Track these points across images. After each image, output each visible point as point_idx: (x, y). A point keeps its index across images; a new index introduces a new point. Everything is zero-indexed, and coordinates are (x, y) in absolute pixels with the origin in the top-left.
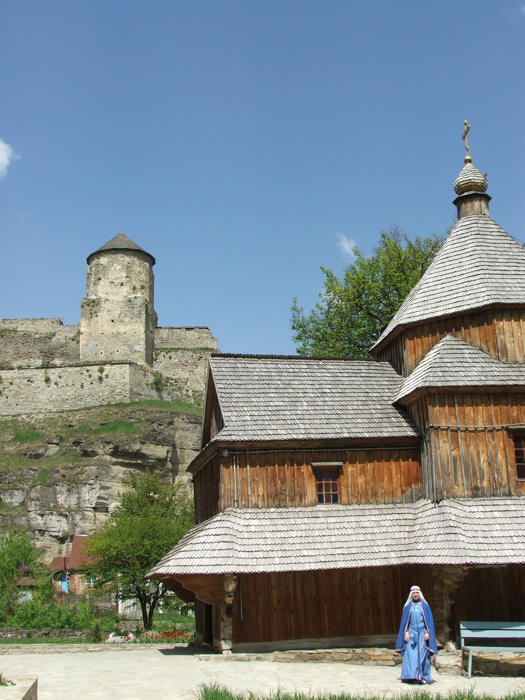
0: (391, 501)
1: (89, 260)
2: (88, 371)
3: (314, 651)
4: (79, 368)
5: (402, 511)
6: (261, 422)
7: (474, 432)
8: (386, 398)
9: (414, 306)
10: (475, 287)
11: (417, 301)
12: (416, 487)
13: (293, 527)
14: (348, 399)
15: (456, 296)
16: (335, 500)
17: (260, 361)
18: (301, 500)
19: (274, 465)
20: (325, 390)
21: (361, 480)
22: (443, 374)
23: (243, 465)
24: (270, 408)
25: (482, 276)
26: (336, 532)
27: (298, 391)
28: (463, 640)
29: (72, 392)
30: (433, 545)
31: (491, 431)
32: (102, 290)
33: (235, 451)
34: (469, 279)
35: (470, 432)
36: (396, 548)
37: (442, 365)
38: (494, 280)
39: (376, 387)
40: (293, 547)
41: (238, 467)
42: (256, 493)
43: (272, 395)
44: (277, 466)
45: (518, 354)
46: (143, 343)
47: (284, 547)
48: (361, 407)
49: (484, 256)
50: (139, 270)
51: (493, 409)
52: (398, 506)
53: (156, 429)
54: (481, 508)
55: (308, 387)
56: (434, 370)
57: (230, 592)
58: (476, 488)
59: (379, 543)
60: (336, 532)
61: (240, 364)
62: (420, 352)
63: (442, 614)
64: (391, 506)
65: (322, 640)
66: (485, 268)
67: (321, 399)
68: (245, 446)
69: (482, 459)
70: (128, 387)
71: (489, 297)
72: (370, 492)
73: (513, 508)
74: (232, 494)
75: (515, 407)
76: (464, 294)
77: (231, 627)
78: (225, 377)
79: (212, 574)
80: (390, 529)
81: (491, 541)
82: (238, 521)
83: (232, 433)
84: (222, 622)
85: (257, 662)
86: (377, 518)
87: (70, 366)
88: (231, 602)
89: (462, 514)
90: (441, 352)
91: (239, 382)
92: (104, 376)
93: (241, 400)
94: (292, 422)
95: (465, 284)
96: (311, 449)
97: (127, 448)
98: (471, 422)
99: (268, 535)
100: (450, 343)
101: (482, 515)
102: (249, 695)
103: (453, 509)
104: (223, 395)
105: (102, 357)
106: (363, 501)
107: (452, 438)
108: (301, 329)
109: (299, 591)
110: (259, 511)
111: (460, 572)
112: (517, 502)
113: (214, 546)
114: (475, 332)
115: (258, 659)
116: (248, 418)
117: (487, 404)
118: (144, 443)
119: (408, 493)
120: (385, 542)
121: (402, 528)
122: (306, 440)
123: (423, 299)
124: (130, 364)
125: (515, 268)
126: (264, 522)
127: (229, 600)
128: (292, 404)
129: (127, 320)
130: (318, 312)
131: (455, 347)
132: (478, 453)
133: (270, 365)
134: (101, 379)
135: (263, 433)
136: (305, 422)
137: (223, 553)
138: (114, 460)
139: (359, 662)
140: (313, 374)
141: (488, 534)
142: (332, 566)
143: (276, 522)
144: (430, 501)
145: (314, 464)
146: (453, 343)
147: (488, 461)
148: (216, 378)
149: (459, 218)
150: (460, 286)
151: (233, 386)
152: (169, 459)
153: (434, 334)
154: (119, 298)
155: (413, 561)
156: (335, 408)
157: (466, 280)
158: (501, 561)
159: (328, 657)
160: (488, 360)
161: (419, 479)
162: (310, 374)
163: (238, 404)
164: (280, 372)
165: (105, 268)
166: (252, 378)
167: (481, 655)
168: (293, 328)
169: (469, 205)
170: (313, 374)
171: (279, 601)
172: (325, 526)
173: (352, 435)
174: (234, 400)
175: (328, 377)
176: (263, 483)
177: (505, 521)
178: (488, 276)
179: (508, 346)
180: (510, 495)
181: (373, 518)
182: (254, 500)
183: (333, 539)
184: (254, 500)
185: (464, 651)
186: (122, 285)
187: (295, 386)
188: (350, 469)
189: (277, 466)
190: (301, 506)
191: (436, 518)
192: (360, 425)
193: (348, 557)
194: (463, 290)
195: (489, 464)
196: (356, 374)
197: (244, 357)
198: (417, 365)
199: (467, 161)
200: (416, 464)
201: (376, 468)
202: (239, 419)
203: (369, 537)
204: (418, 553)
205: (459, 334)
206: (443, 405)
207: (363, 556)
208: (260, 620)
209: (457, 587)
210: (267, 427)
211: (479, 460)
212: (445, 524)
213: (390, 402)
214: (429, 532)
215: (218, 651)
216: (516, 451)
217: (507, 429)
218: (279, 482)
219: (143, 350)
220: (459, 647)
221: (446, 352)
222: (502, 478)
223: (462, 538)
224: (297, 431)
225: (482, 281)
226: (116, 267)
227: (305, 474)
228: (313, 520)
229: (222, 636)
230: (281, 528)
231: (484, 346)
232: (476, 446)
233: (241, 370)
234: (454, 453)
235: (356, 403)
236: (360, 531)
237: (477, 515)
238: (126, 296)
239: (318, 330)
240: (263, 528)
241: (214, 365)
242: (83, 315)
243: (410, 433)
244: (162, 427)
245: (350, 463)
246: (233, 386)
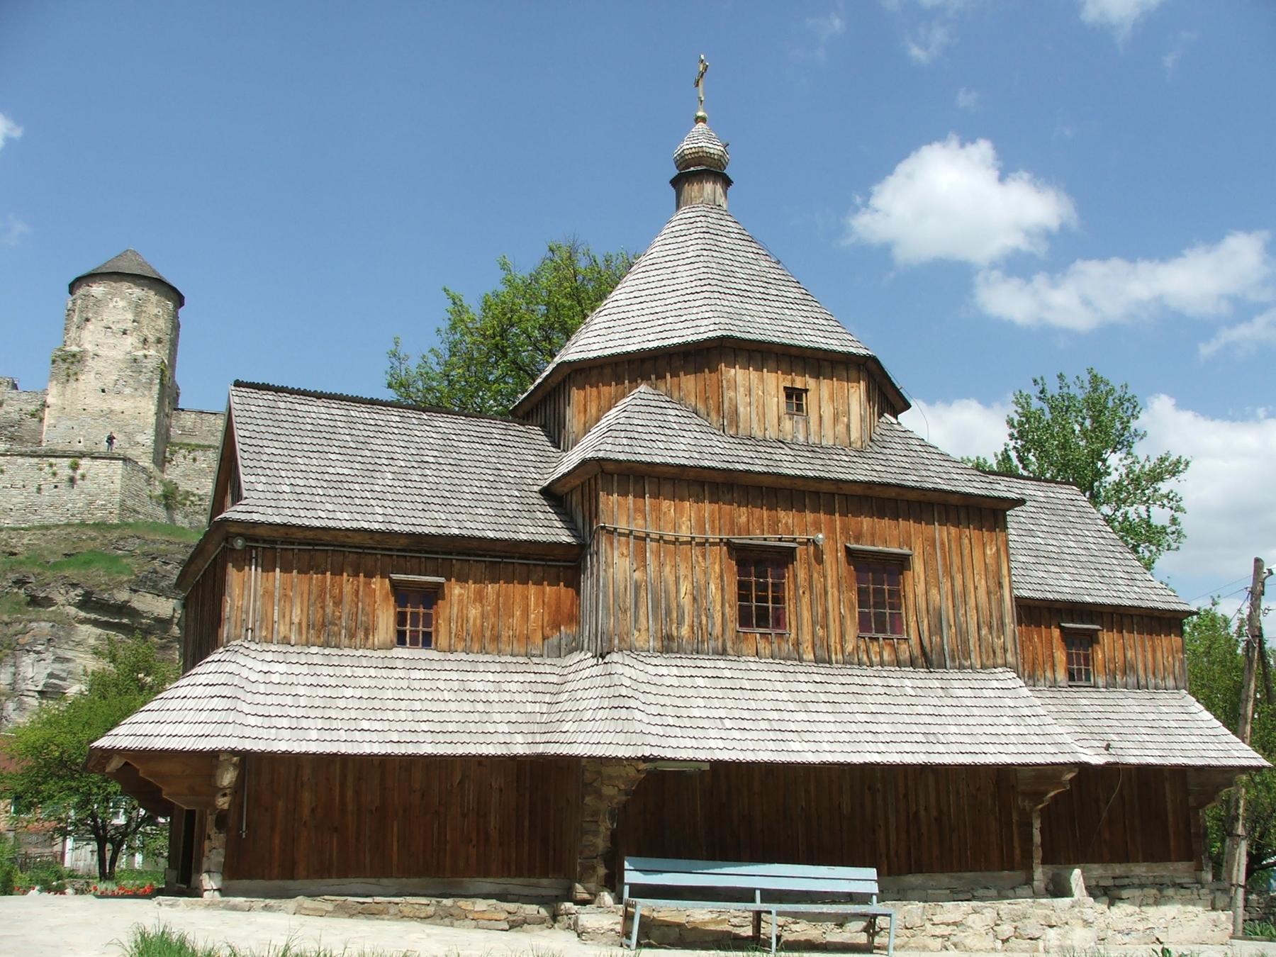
0: (523, 651)
1: (73, 287)
2: (51, 465)
3: (369, 900)
4: (36, 460)
5: (541, 669)
6: (308, 498)
7: (674, 543)
8: (530, 482)
9: (590, 334)
10: (695, 310)
11: (597, 327)
12: (569, 631)
13: (347, 682)
14: (465, 476)
15: (661, 322)
16: (427, 641)
17: (319, 402)
18: (367, 637)
19: (324, 573)
20: (426, 459)
21: (474, 612)
22: (630, 442)
23: (268, 568)
24: (327, 477)
25: (707, 295)
26: (423, 695)
27: (379, 454)
28: (627, 889)
29: (21, 499)
30: (589, 726)
31: (702, 544)
32: (89, 338)
33: (257, 541)
34: (686, 298)
35: (666, 542)
36: (525, 728)
37: (629, 428)
38: (726, 303)
39: (514, 462)
40: (345, 714)
41: (259, 570)
42: (287, 619)
43: (333, 457)
44: (328, 574)
45: (755, 425)
46: (151, 432)
47: (328, 713)
48: (485, 491)
49: (714, 265)
50: (156, 311)
51: (707, 508)
52: (535, 660)
53: (158, 569)
54: (675, 671)
55: (398, 450)
56: (615, 434)
57: (225, 788)
58: (670, 637)
59: (497, 717)
60: (423, 695)
61: (284, 403)
62: (593, 410)
63: (595, 846)
64: (522, 660)
65: (385, 881)
66: (713, 282)
67: (419, 472)
68: (275, 534)
69: (683, 590)
70: (117, 498)
71: (716, 327)
72: (488, 634)
73: (728, 673)
74: (244, 616)
75: (743, 509)
76: (676, 319)
77: (222, 851)
78: (254, 421)
79: (194, 751)
80: (517, 697)
81: (687, 722)
82: (250, 663)
83: (255, 509)
84: (207, 842)
85: (264, 913)
86: (497, 677)
87: (22, 455)
88: (226, 806)
89: (642, 677)
90: (629, 408)
91: (278, 431)
92: (78, 477)
93: (278, 458)
94: (363, 502)
95: (679, 305)
96: (391, 550)
97: (106, 596)
98: (670, 526)
99: (301, 690)
100: (645, 396)
101: (675, 682)
102: (228, 951)
103: (624, 668)
104: (245, 448)
105: (80, 447)
106: (476, 647)
107: (635, 550)
108: (399, 384)
109: (350, 793)
110: (291, 649)
111: (632, 773)
112: (735, 665)
113: (203, 704)
114: (689, 382)
115: (267, 908)
116: (287, 489)
117: (699, 499)
118: (135, 591)
119: (554, 640)
120: (507, 718)
121: (539, 697)
122: (383, 532)
123: (606, 325)
124: (125, 460)
125: (762, 290)
126: (297, 669)
127: (223, 802)
128: (367, 473)
129: (127, 391)
130: (432, 360)
131: (653, 403)
132: (677, 579)
133: (336, 410)
134: (72, 480)
135: (309, 514)
136: (385, 503)
137: (216, 716)
138: (82, 614)
139: (447, 921)
140: (408, 432)
141: (684, 712)
142: (410, 750)
143: (319, 670)
144: (589, 654)
145: (395, 576)
146: (651, 397)
147: (692, 594)
148: (238, 420)
149: (678, 207)
150: (670, 307)
151: (266, 435)
152: (176, 620)
153: (619, 381)
154: (119, 354)
155: (552, 750)
156: (440, 487)
157: (681, 299)
158: (702, 755)
159: (392, 911)
160: (705, 429)
161: (574, 618)
162: (403, 431)
163: (271, 465)
164: (352, 422)
165: (98, 303)
166: (302, 426)
167: (655, 914)
168: (390, 386)
169: (696, 187)
170: (408, 432)
171: (313, 811)
172: (404, 684)
173: (464, 532)
174: (265, 457)
175: (434, 438)
176: (302, 603)
177: (713, 693)
178: (716, 295)
179: (741, 409)
180: (724, 652)
181: (490, 677)
182: (282, 629)
183: (418, 705)
184: (282, 629)
185: (627, 905)
186: (125, 333)
187: (375, 447)
188: (456, 590)
189: (328, 574)
190: (365, 647)
191: (598, 682)
192: (481, 518)
193: (441, 738)
194: (674, 313)
195: (694, 599)
196: (482, 439)
197: (292, 392)
198: (586, 431)
199: (698, 120)
200: (571, 591)
201: (503, 592)
202: (270, 488)
203: (480, 707)
204: (562, 738)
205: (661, 384)
206: (624, 494)
207: (466, 738)
208: (277, 841)
209: (624, 798)
210: (319, 506)
211: (678, 591)
212: (612, 691)
213: (536, 488)
214: (583, 705)
215: (196, 892)
216: (739, 582)
217: (728, 543)
218: (330, 603)
219: (149, 443)
220: (619, 899)
221: (637, 409)
222: (713, 624)
223: (638, 715)
224: (370, 517)
225: (706, 301)
226: (118, 304)
227: (378, 592)
228: (385, 673)
229: (205, 867)
230: (327, 681)
231: (701, 407)
232: (675, 566)
233: (284, 412)
234: (637, 575)
235: (477, 483)
236: (466, 696)
237: (668, 681)
238: (129, 353)
239: (430, 389)
240: (293, 679)
241: (237, 400)
242: (53, 376)
243: (565, 537)
244: (168, 567)
245: (458, 580)
246: (266, 435)
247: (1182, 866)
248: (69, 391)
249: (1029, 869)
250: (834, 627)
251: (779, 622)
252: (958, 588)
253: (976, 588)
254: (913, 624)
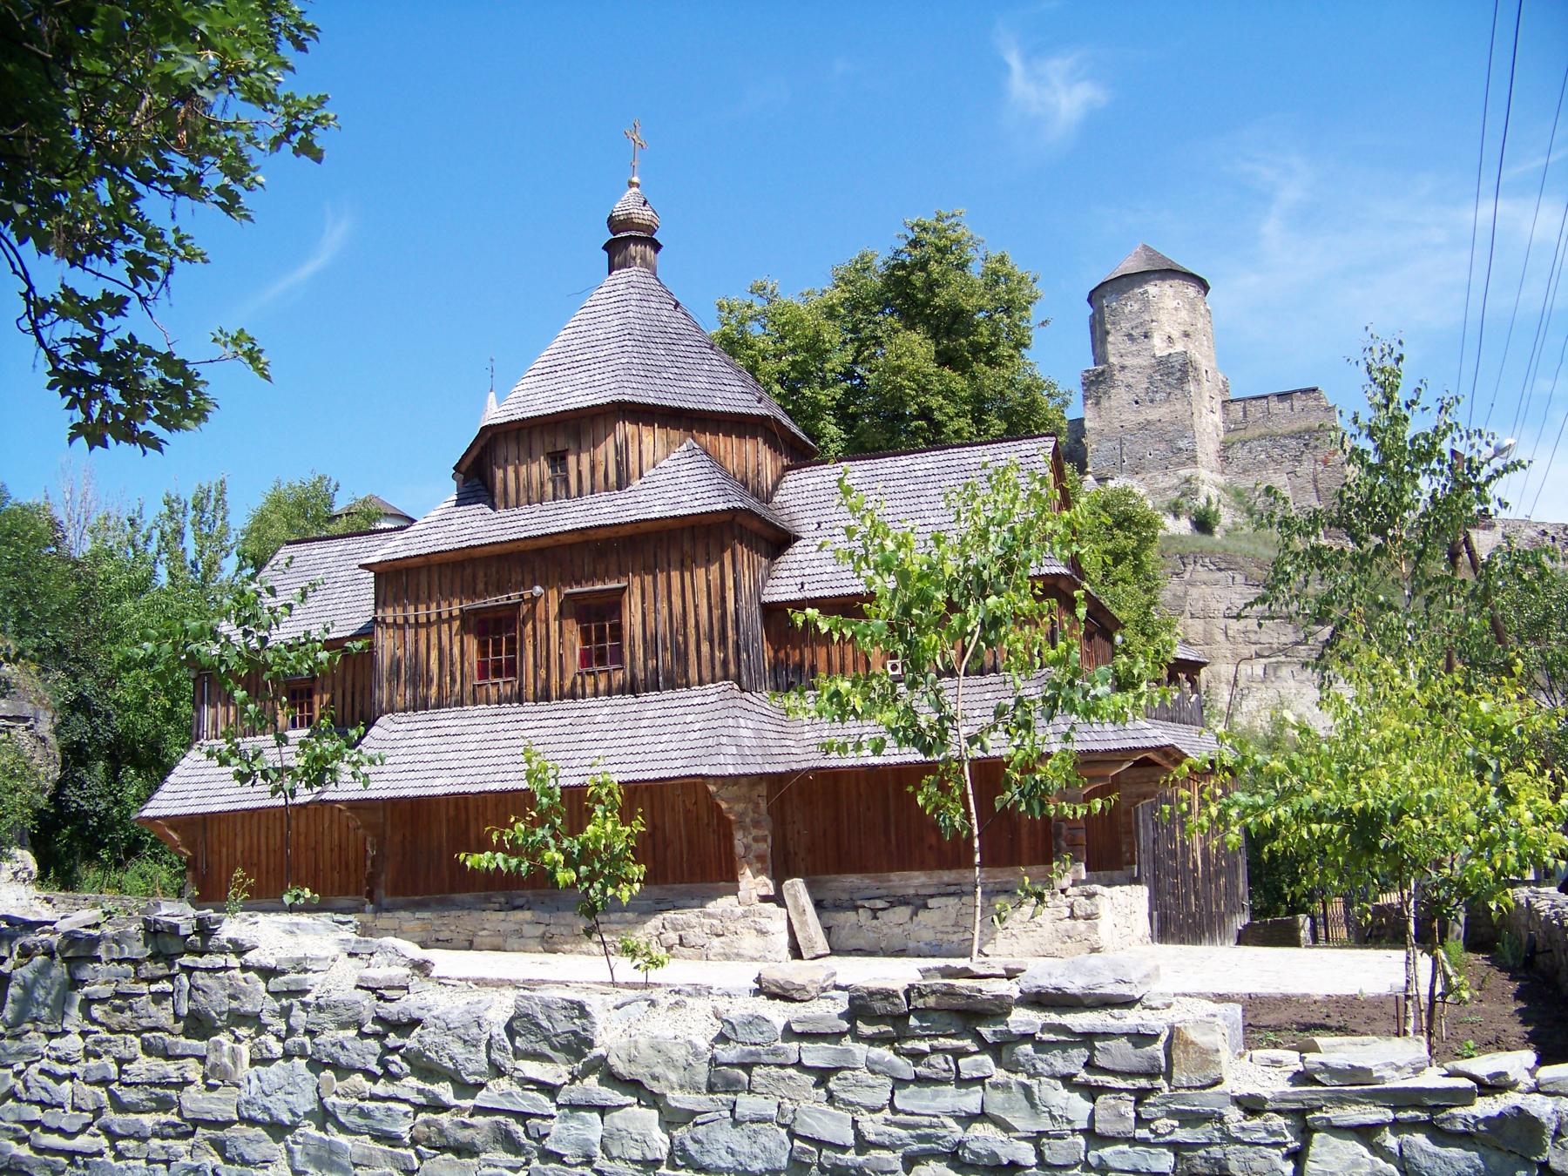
50: (1175, 304)
109: (263, 840)
129: (1157, 397)
154: (1144, 361)
199: (631, 184)
253: (696, 607)
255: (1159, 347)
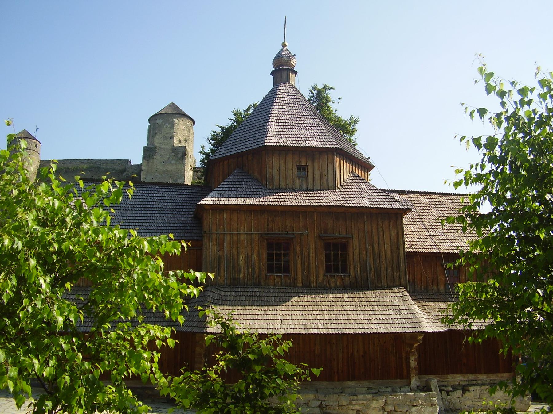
58: (234, 279)
147: (245, 260)
211: (238, 258)
234: (219, 253)
247: (505, 375)
248: (150, 164)
249: (409, 378)
250: (313, 271)
251: (287, 270)
252: (376, 250)
253: (385, 251)
254: (352, 268)
255: (176, 143)
